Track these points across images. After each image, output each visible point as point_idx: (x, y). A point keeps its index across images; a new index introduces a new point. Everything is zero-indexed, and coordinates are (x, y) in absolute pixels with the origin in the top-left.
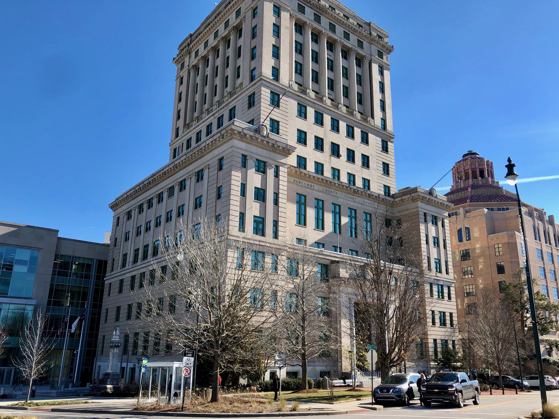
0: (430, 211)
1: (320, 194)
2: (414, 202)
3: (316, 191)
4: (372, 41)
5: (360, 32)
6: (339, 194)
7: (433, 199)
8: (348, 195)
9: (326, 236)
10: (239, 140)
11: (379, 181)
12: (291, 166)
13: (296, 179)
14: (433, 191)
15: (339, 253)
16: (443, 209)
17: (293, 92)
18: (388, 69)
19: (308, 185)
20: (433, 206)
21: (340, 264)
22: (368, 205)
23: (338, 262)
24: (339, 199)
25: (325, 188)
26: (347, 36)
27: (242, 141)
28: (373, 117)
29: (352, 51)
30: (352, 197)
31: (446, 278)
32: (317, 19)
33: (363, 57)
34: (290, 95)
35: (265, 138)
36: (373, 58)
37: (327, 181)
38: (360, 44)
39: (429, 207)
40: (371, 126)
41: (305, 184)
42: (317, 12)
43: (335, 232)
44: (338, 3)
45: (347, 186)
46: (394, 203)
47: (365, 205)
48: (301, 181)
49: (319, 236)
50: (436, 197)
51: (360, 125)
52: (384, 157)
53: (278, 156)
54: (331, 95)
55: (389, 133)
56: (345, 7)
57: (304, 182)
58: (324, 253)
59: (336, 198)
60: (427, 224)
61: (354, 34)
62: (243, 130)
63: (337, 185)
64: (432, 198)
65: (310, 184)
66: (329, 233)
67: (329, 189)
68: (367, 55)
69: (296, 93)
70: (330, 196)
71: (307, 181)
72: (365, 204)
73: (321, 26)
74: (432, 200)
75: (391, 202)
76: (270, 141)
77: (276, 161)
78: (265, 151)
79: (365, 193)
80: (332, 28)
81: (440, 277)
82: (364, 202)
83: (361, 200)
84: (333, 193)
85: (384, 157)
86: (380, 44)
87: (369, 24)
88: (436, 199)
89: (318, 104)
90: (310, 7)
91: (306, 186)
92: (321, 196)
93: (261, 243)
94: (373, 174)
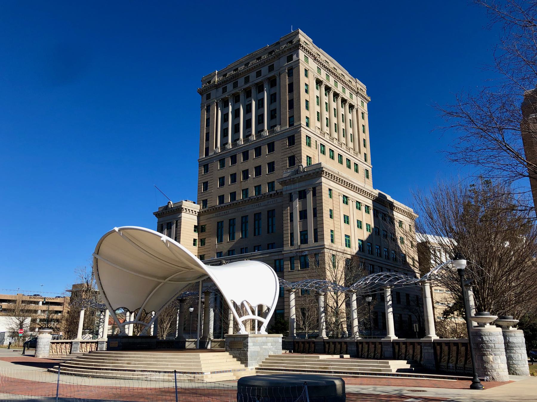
8: (253, 204)
13: (217, 213)
22: (272, 203)
25: (236, 209)
40: (278, 132)
71: (224, 210)
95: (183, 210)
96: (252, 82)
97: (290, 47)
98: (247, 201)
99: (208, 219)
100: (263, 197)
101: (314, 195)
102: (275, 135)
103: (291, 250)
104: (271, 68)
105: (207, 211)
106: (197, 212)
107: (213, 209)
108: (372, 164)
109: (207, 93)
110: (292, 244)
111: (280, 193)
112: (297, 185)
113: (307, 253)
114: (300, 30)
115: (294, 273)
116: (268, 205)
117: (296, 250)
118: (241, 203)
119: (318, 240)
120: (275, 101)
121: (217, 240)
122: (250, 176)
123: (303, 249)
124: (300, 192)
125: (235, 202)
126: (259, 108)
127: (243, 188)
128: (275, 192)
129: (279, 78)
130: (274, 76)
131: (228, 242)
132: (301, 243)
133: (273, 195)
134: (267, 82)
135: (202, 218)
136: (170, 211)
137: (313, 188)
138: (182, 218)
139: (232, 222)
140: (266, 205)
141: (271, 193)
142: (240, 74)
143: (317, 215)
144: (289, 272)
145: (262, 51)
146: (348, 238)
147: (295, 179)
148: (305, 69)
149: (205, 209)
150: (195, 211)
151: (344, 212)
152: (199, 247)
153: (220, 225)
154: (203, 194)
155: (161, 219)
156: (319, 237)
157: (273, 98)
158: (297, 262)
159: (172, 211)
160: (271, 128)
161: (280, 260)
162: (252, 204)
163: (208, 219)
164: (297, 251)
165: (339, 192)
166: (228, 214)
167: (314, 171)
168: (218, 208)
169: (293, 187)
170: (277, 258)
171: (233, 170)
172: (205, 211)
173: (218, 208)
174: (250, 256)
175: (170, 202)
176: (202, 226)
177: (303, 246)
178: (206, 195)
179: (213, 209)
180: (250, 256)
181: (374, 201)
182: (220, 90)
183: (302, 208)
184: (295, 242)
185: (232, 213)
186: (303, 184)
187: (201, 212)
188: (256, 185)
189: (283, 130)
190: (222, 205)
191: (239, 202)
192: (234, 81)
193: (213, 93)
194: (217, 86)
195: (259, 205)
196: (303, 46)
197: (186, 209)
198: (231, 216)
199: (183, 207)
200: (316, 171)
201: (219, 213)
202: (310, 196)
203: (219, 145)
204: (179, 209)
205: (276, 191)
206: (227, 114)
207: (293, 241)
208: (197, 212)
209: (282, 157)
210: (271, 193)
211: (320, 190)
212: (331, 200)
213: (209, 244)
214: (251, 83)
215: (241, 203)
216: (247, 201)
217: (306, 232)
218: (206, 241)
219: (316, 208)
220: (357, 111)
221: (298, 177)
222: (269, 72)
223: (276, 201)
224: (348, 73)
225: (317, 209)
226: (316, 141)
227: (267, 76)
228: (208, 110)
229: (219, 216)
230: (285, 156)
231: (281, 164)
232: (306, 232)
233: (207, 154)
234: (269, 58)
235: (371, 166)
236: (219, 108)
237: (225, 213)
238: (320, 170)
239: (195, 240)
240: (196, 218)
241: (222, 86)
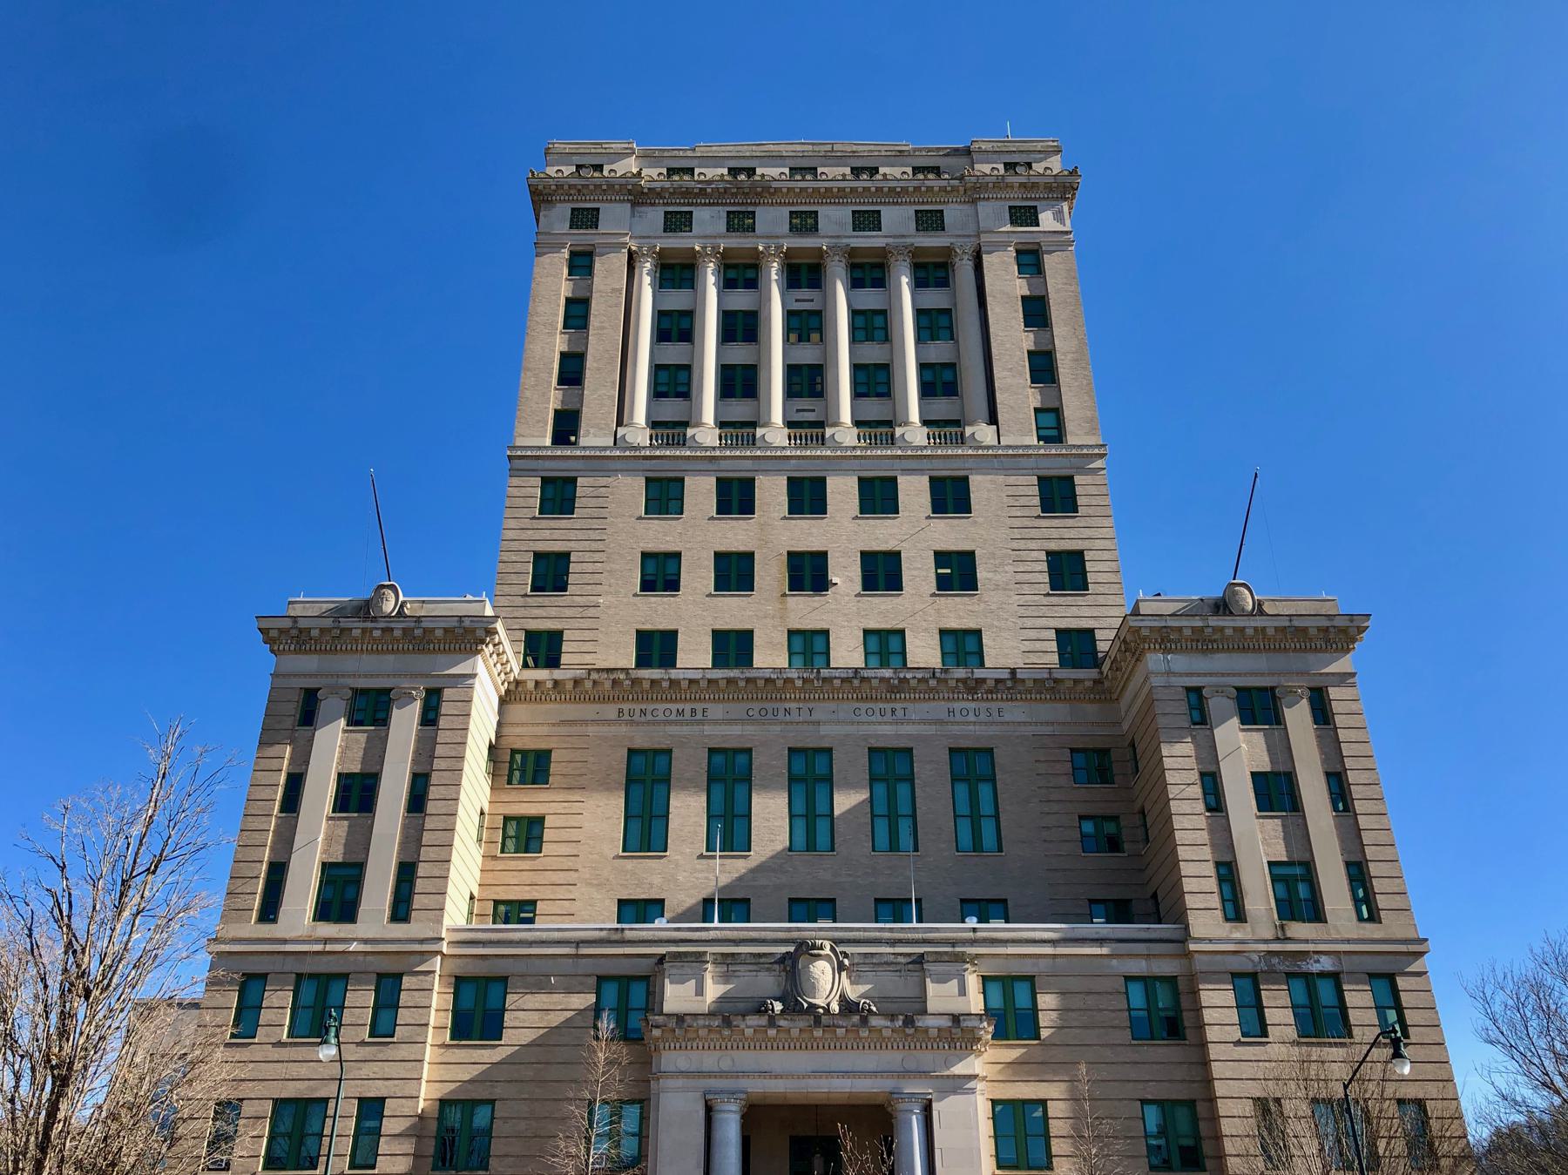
0: (1223, 675)
1: (736, 730)
2: (1137, 660)
3: (716, 722)
4: (974, 192)
5: (917, 189)
6: (822, 711)
7: (1221, 624)
8: (864, 706)
9: (753, 871)
10: (296, 652)
11: (1029, 623)
12: (590, 670)
13: (626, 707)
14: (1235, 593)
15: (716, 924)
16: (1316, 650)
17: (627, 453)
18: (1063, 246)
19: (643, 712)
20: (1244, 650)
21: (666, 965)
22: (971, 718)
23: (662, 959)
24: (822, 728)
25: (757, 706)
26: (867, 221)
27: (305, 652)
28: (993, 419)
29: (890, 252)
30: (888, 706)
31: (1348, 941)
32: (740, 222)
33: (948, 251)
34: (619, 465)
35: (376, 621)
36: (984, 238)
37: (768, 680)
38: (930, 221)
39: (1200, 663)
41: (667, 713)
42: (739, 204)
43: (811, 846)
44: (829, 148)
45: (842, 675)
46: (1107, 684)
47: (953, 723)
48: (651, 707)
49: (725, 871)
50: (1259, 609)
51: (925, 464)
52: (1055, 533)
53: (442, 658)
54: (814, 410)
55: (1074, 446)
56: (855, 148)
57: (661, 707)
58: (629, 935)
59: (811, 727)
60: (1211, 729)
61: (897, 203)
62: (296, 622)
63: (799, 683)
64: (1240, 622)
65: (688, 707)
66: (772, 857)
67: (776, 705)
68: (958, 242)
69: (637, 453)
70: (778, 728)
72: (958, 717)
73: (758, 237)
74: (1222, 629)
75: (1088, 684)
76: (393, 625)
77: (427, 676)
78: (391, 657)
79: (946, 680)
80: (805, 223)
81: (1307, 941)
82: (951, 712)
83: (938, 708)
84: (795, 713)
85: (1055, 533)
86: (1010, 186)
87: (967, 152)
88: (1259, 622)
89: (725, 458)
90: (710, 204)
91: (673, 717)
92: (731, 734)
93: (329, 948)
94: (993, 607)
99: (563, 722)
105: (569, 686)
107: (615, 682)
113: (1326, 964)
117: (1266, 941)
145: (883, 154)
162: (857, 705)
163: (563, 722)
167: (1325, 623)
170: (1138, 967)
179: (615, 682)
186: (1280, 661)
188: (873, 625)
192: (734, 204)
195: (900, 713)
201: (637, 707)
204: (473, 631)
209: (1015, 545)
227: (909, 241)
229: (638, 724)
237: (680, 713)
238: (1355, 624)
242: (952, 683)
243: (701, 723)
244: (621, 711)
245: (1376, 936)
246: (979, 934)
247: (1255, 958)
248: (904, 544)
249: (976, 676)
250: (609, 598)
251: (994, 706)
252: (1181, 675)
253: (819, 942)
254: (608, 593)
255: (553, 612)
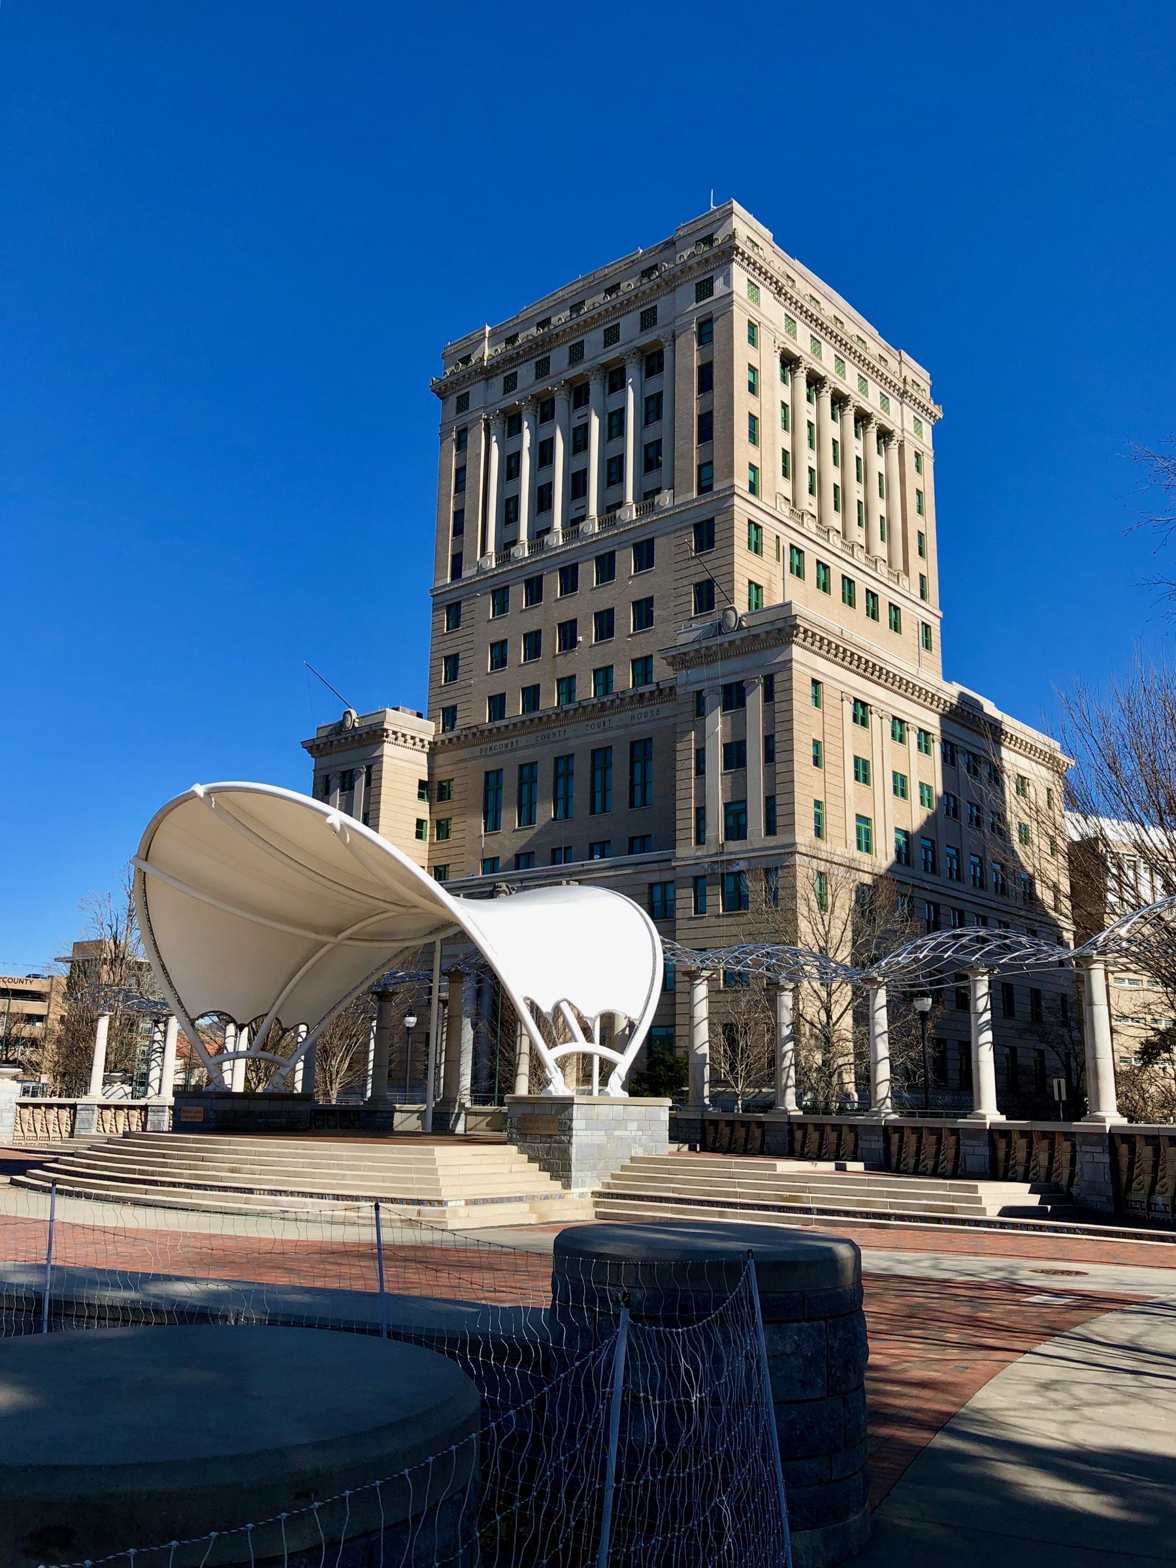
3: (522, 748)
13: (483, 746)
16: (774, 646)
22: (643, 719)
71: (500, 740)
72: (636, 720)
83: (625, 717)
95: (387, 736)
96: (590, 360)
97: (705, 256)
98: (572, 712)
100: (618, 702)
101: (769, 696)
102: (655, 518)
103: (698, 858)
104: (649, 319)
106: (426, 743)
107: (474, 734)
108: (941, 608)
109: (458, 391)
110: (700, 841)
111: (668, 690)
112: (719, 668)
113: (742, 866)
114: (736, 206)
115: (705, 922)
116: (633, 725)
117: (711, 856)
118: (554, 717)
119: (778, 829)
120: (659, 417)
121: (485, 824)
122: (580, 638)
123: (731, 853)
124: (727, 689)
125: (537, 714)
126: (610, 438)
127: (560, 676)
128: (652, 687)
129: (671, 348)
130: (657, 343)
131: (515, 831)
132: (728, 836)
133: (647, 695)
134: (634, 360)
135: (440, 759)
136: (350, 739)
137: (765, 677)
138: (385, 759)
139: (527, 773)
140: (626, 726)
141: (641, 690)
142: (557, 335)
143: (777, 755)
144: (691, 918)
145: (623, 268)
146: (864, 826)
147: (714, 648)
148: (749, 321)
149: (450, 735)
150: (422, 740)
151: (855, 749)
152: (431, 844)
153: (492, 780)
154: (444, 690)
155: (325, 761)
156: (780, 821)
157: (652, 409)
158: (715, 892)
159: (357, 737)
160: (646, 497)
161: (664, 885)
162: (587, 723)
164: (715, 859)
165: (843, 688)
166: (515, 750)
167: (769, 628)
168: (486, 733)
169: (705, 672)
170: (655, 878)
171: (532, 620)
172: (450, 740)
173: (486, 733)
174: (579, 873)
175: (349, 712)
176: (440, 783)
177: (734, 846)
178: (453, 694)
180: (579, 873)
181: (944, 717)
182: (498, 382)
183: (733, 736)
184: (709, 834)
185: (527, 747)
187: (439, 744)
188: (598, 666)
189: (681, 505)
190: (499, 723)
191: (549, 716)
193: (477, 393)
194: (487, 373)
195: (607, 724)
196: (743, 254)
197: (395, 733)
198: (524, 756)
199: (386, 726)
200: (776, 627)
202: (755, 699)
203: (491, 547)
204: (375, 731)
205: (658, 684)
206: (518, 456)
207: (704, 831)
208: (426, 743)
209: (675, 585)
210: (641, 690)
211: (786, 684)
212: (817, 712)
213: (460, 835)
214: (587, 364)
215: (554, 717)
216: (572, 712)
217: (742, 806)
218: (453, 827)
219: (773, 736)
220: (901, 447)
221: (721, 645)
222: (642, 330)
223: (655, 713)
224: (876, 333)
225: (776, 740)
226: (778, 537)
227: (634, 343)
228: (461, 444)
230: (685, 582)
231: (671, 604)
232: (742, 806)
233: (456, 573)
234: (642, 289)
235: (940, 614)
236: (494, 438)
237: (507, 746)
239: (420, 823)
240: (423, 758)
241: (503, 372)
242: (628, 700)
243: (513, 750)
244: (481, 750)
245: (772, 845)
246: (585, 868)
247: (706, 866)
248: (616, 602)
249: (640, 692)
250: (477, 679)
251: (654, 708)
252: (694, 683)
253: (499, 884)
254: (475, 676)
255: (453, 694)
